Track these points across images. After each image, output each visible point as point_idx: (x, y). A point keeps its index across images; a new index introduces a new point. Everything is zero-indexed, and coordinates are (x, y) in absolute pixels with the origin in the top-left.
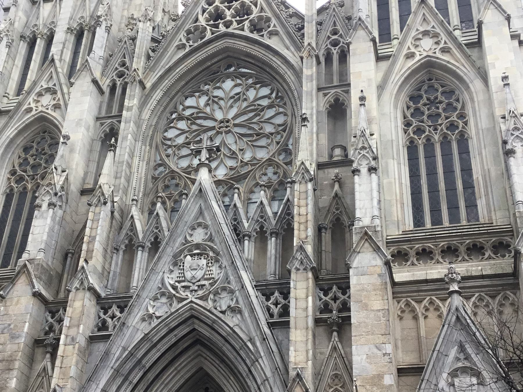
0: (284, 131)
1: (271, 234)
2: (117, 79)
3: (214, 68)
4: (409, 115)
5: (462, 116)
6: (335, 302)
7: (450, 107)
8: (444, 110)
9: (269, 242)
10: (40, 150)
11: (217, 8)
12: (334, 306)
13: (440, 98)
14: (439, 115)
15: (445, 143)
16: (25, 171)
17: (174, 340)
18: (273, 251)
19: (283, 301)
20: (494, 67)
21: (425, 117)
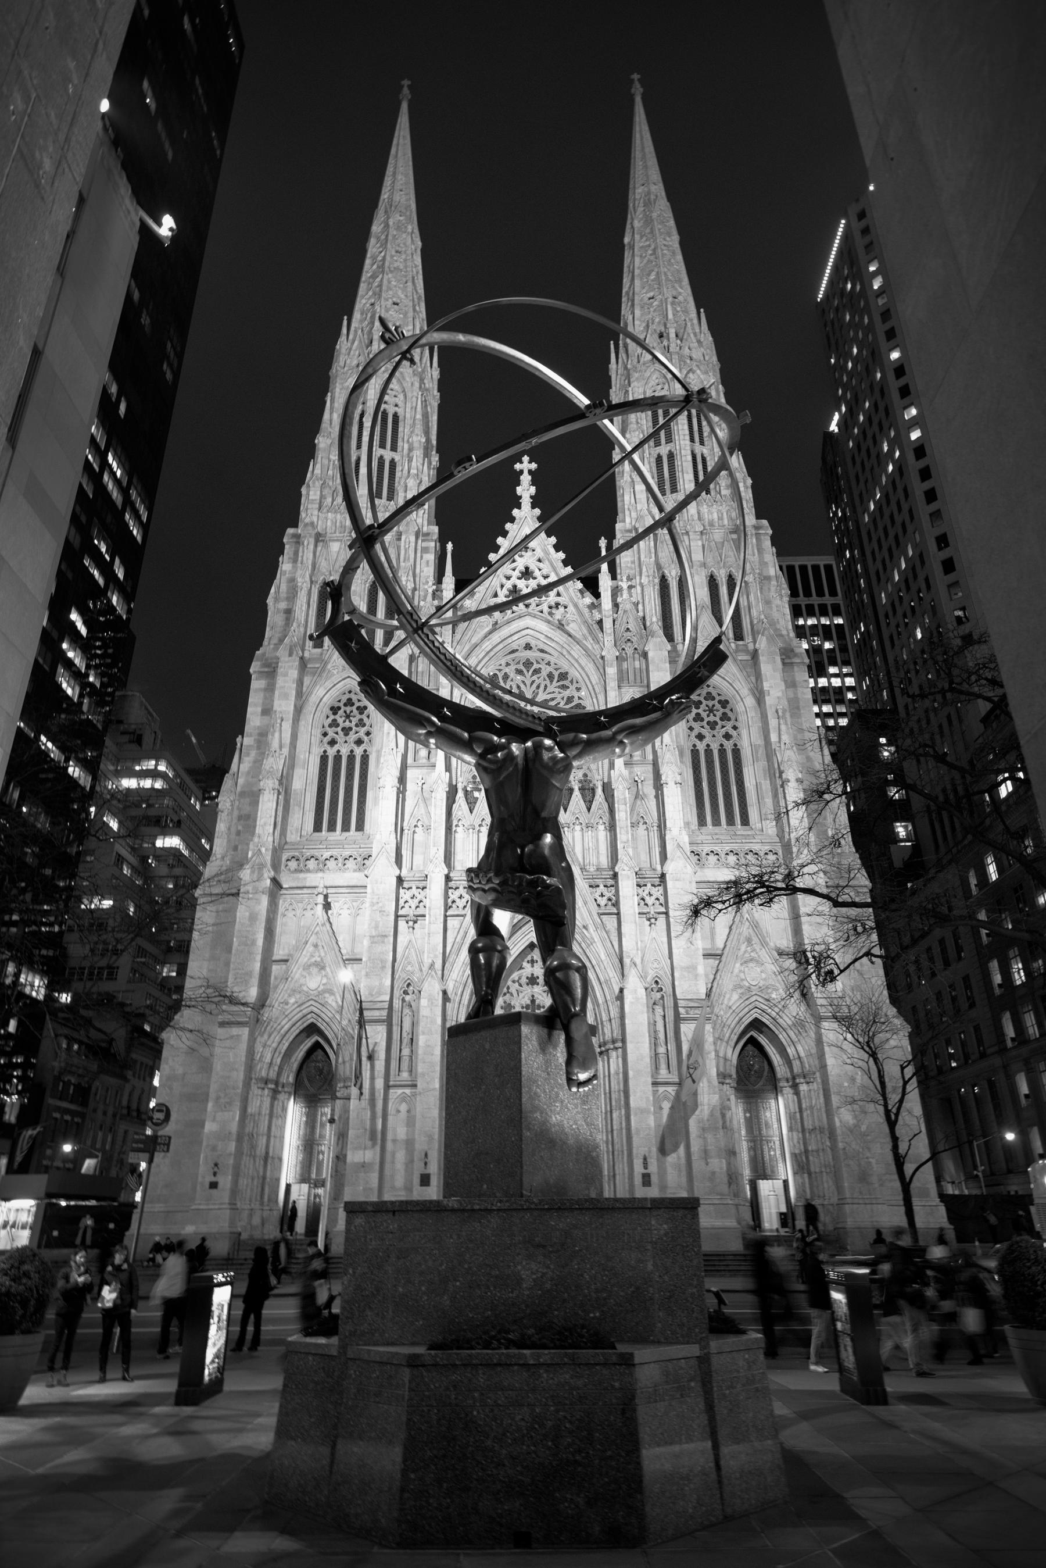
3: (514, 646)
5: (735, 728)
7: (725, 717)
8: (722, 719)
11: (515, 586)
13: (718, 706)
14: (716, 723)
15: (722, 751)
16: (337, 733)
21: (705, 723)
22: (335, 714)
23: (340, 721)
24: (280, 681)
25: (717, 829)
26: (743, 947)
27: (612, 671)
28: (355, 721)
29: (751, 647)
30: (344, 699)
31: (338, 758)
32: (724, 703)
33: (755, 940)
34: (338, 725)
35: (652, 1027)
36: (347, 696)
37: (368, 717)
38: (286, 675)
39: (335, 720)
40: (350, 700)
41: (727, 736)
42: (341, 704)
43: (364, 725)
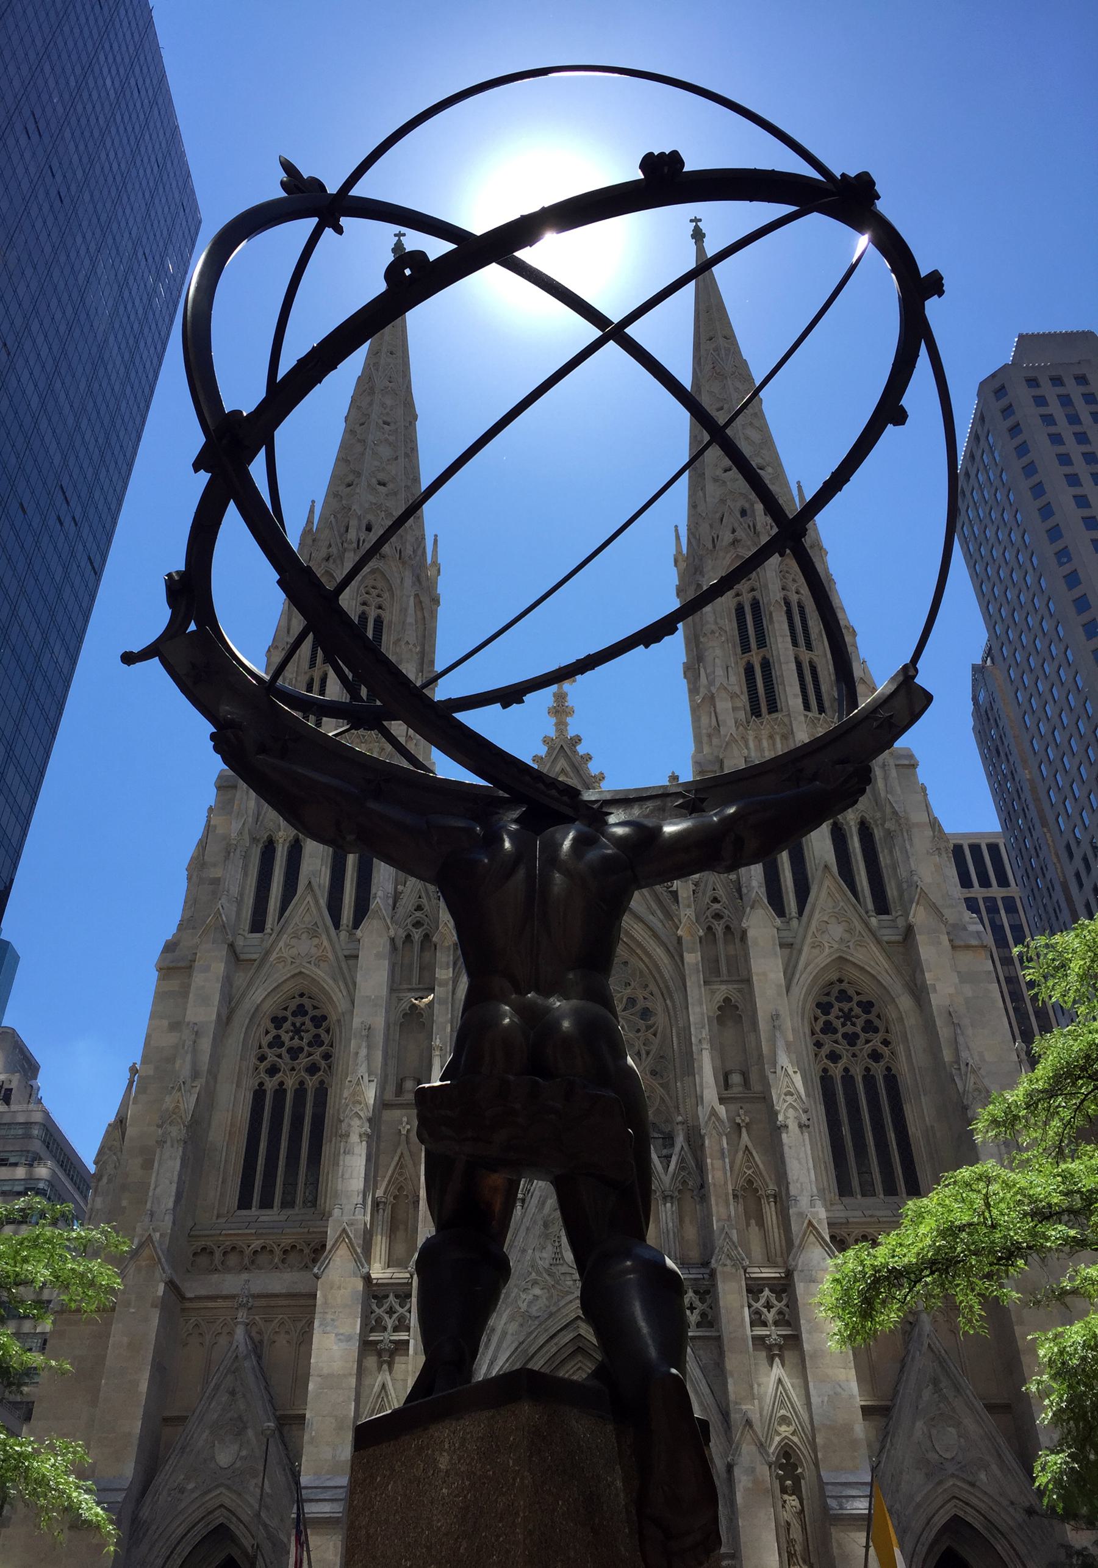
0: (655, 1035)
1: (665, 1198)
2: (414, 930)
4: (818, 1029)
5: (886, 1043)
6: (769, 1311)
9: (661, 1208)
10: (298, 1025)
12: (770, 1316)
13: (857, 1010)
14: (856, 1036)
15: (869, 1079)
16: (280, 1056)
17: (554, 1350)
18: (671, 1225)
19: (700, 1305)
20: (935, 991)
21: (839, 1035)
22: (278, 1027)
23: (285, 1038)
24: (198, 979)
25: (869, 1201)
26: (927, 1394)
27: (692, 958)
28: (307, 1037)
29: (901, 922)
30: (293, 1006)
31: (280, 1092)
32: (867, 1006)
33: (944, 1383)
34: (282, 1045)
35: (782, 1532)
36: (298, 1001)
37: (328, 1031)
38: (207, 969)
39: (277, 1037)
40: (301, 1006)
41: (876, 1056)
42: (288, 1013)
43: (322, 1044)
